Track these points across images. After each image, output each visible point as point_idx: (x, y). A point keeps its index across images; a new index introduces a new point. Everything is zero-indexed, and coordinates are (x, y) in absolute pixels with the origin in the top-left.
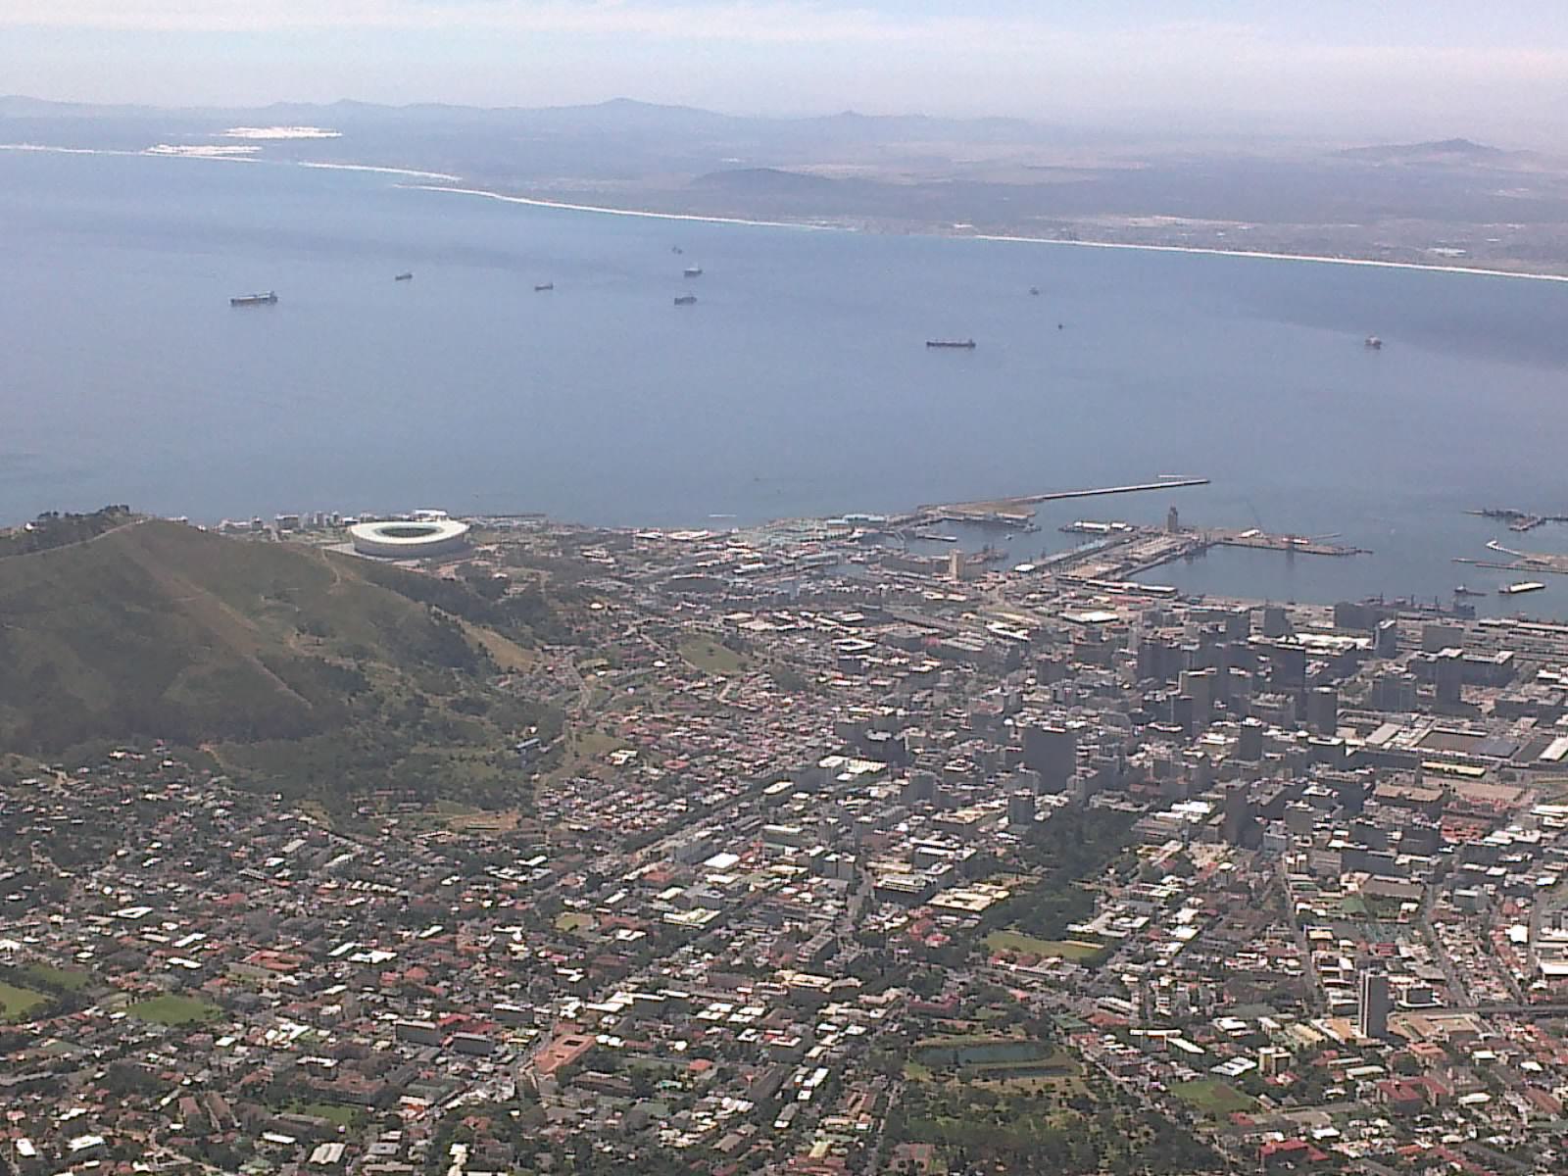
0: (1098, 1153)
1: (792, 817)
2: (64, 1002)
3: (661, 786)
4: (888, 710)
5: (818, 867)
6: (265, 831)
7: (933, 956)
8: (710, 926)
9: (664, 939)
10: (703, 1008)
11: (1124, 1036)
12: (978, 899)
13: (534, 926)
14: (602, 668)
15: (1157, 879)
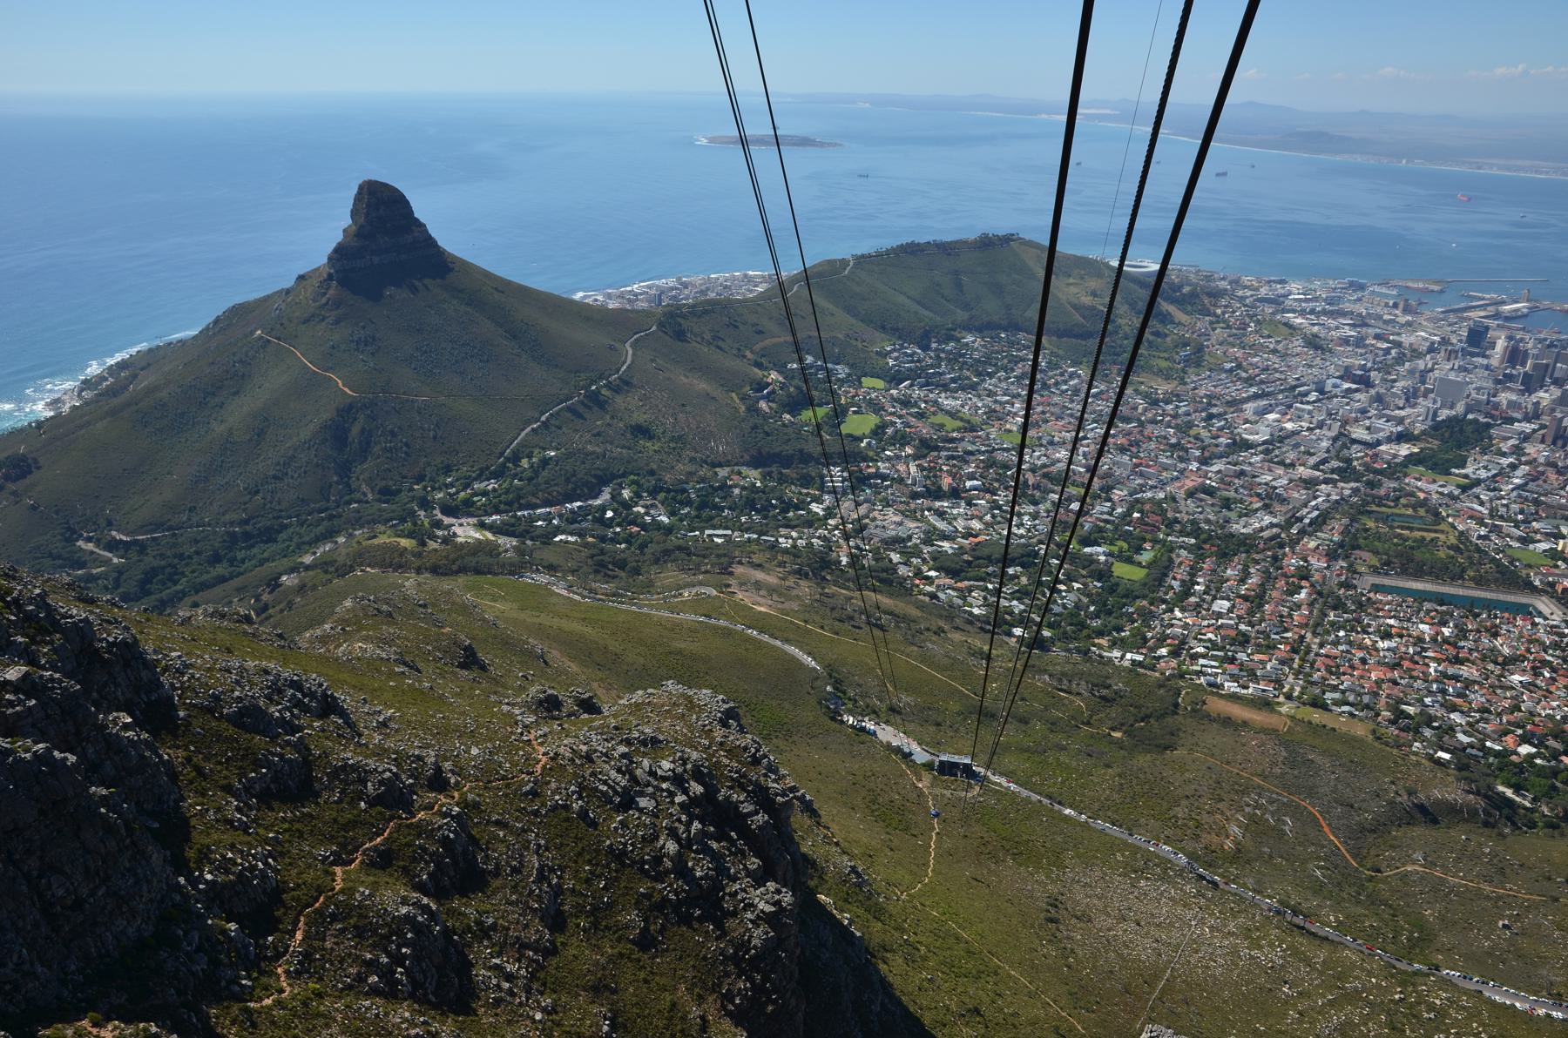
0: (1464, 570)
1: (1308, 403)
2: (973, 429)
5: (1321, 425)
7: (1377, 472)
8: (1265, 442)
11: (1481, 522)
12: (1404, 450)
15: (1504, 455)
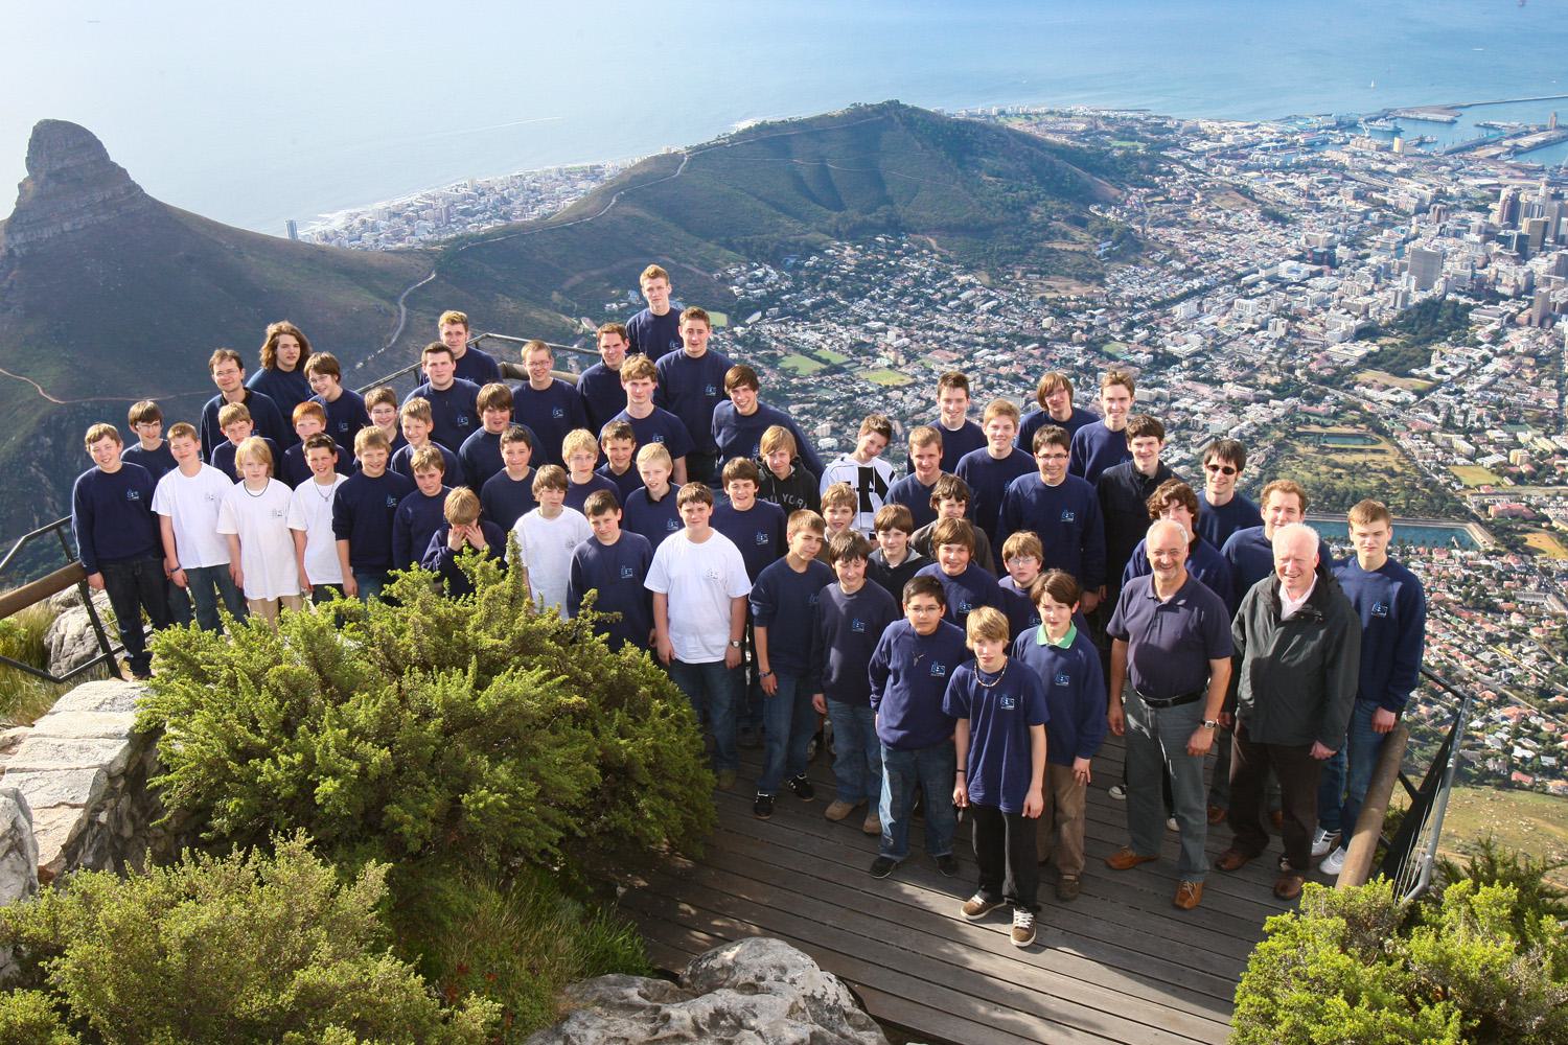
3: (1180, 273)
4: (1330, 235)
6: (951, 285)
9: (1164, 361)
10: (1176, 400)
12: (1361, 349)
13: (1092, 347)
14: (1161, 202)
